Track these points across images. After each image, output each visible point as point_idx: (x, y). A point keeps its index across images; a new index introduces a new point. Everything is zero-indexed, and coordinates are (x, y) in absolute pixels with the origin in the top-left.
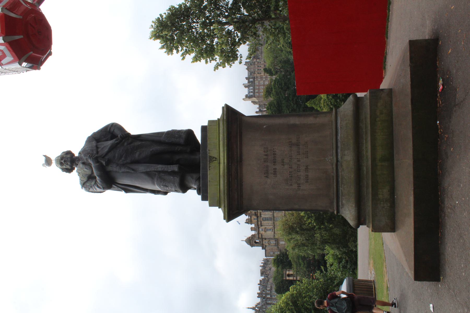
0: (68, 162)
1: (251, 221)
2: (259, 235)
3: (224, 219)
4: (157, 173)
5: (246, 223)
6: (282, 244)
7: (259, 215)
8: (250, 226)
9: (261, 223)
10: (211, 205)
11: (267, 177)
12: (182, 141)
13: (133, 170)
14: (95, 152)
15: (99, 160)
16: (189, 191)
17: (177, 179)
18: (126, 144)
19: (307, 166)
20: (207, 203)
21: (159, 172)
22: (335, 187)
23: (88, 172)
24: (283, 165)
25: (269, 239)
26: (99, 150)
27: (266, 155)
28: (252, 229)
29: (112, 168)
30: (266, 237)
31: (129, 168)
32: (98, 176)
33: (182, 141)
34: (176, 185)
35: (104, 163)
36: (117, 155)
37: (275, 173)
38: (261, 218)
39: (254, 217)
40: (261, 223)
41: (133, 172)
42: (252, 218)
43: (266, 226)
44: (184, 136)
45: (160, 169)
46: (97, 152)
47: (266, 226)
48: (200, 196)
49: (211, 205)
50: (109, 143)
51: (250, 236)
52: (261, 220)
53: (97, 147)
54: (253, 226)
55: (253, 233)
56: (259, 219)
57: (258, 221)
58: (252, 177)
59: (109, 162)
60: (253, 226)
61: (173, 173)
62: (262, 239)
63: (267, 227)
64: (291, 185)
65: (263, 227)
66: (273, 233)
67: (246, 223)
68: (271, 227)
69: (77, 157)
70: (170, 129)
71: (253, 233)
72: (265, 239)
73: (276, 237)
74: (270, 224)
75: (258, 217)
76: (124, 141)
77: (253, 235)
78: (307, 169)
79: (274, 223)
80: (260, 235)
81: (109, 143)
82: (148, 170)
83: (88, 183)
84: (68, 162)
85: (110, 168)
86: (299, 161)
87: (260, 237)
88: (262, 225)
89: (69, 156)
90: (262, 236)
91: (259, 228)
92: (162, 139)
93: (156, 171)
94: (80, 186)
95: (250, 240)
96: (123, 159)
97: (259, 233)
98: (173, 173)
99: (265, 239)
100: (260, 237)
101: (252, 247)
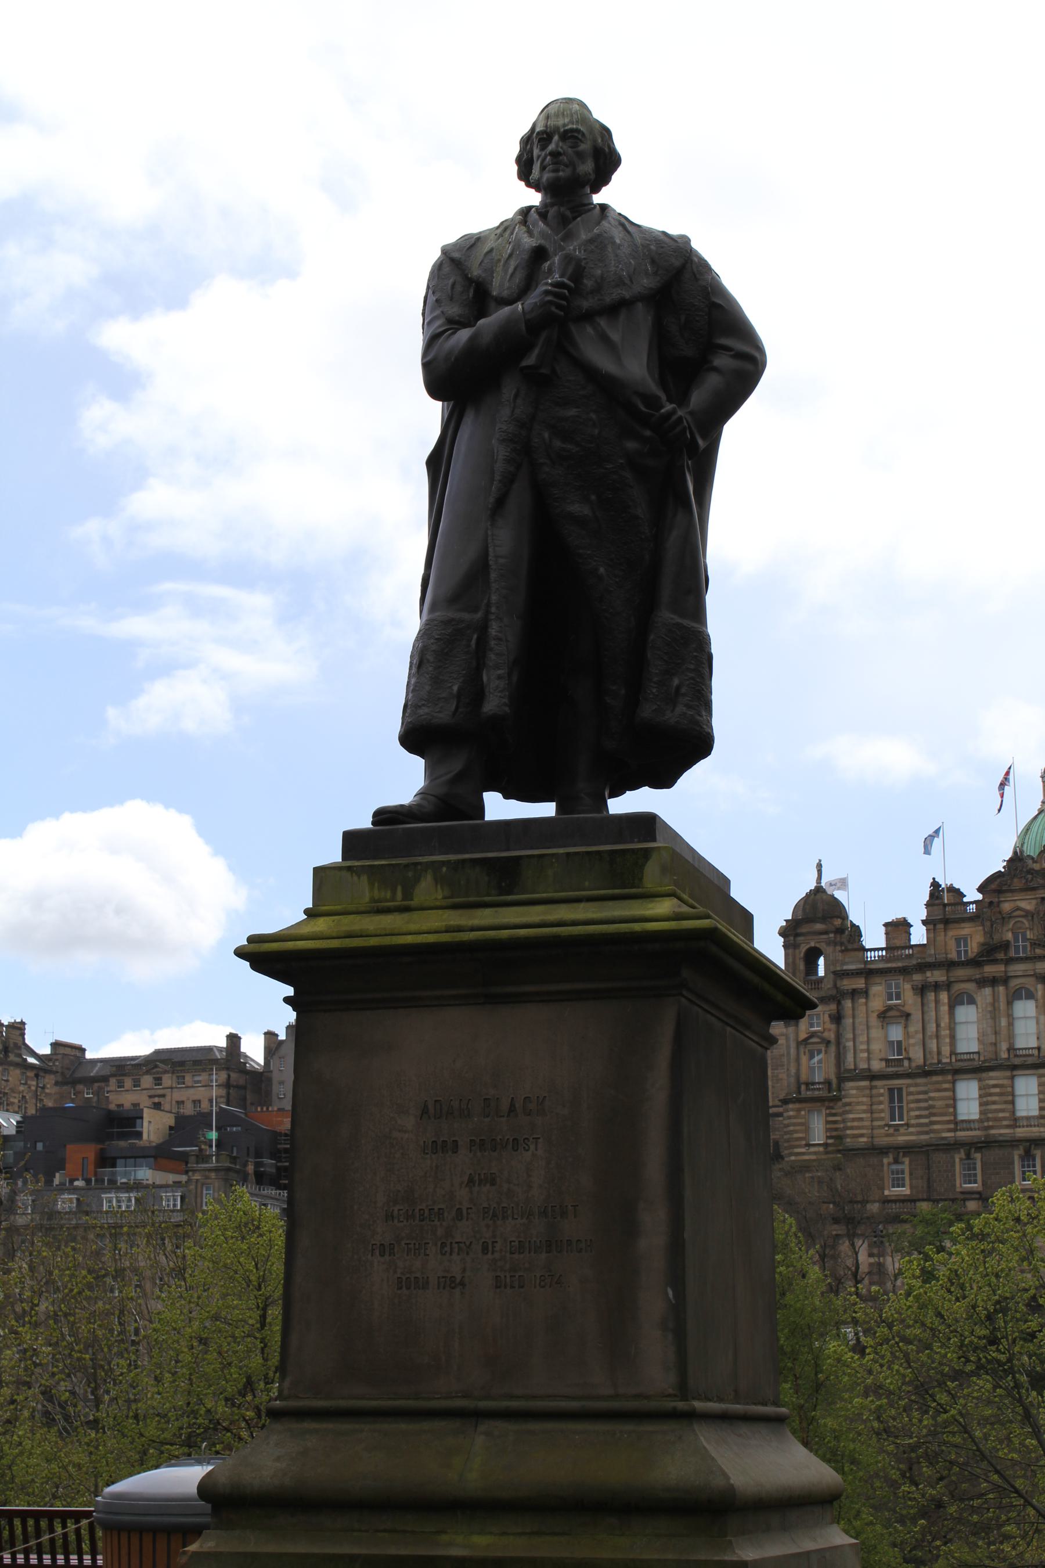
0: (569, 154)
1: (947, 922)
2: (857, 973)
3: (251, 939)
4: (479, 615)
5: (935, 885)
6: (807, 1129)
7: (990, 970)
8: (916, 914)
9: (937, 987)
10: (321, 874)
11: (425, 1111)
12: (647, 711)
13: (500, 503)
14: (586, 304)
15: (544, 335)
16: (418, 763)
17: (443, 714)
18: (631, 445)
19: (462, 1284)
20: (334, 855)
21: (483, 628)
22: (374, 1403)
23: (500, 284)
24: (471, 1181)
25: (839, 1036)
26: (602, 322)
27: (512, 1109)
28: (898, 928)
29: (509, 401)
30: (848, 1021)
31: (509, 481)
32: (472, 339)
33: (647, 711)
34: (426, 710)
35: (531, 360)
36: (572, 412)
37: (442, 1147)
38: (970, 987)
39: (975, 938)
40: (937, 987)
41: (492, 500)
42: (966, 929)
43: (916, 1015)
44: (674, 715)
45: (494, 630)
46: (588, 317)
47: (916, 1015)
48: (365, 822)
49: (321, 874)
50: (633, 365)
51: (855, 916)
52: (957, 987)
53: (613, 310)
54: (919, 935)
55: (874, 938)
56: (961, 973)
57: (950, 965)
58: (429, 1048)
59: (539, 382)
60: (919, 935)
61: (474, 692)
62: (837, 997)
63: (915, 1026)
64: (389, 1217)
65: (909, 999)
66: (877, 1066)
67: (935, 885)
68: (917, 1055)
69: (583, 207)
70: (715, 649)
71: (874, 938)
72: (837, 1018)
73: (853, 1090)
74: (933, 1045)
75: (975, 963)
76: (648, 433)
77: (856, 932)
78: (450, 1283)
79: (942, 1072)
80: (860, 983)
81: (633, 365)
82: (493, 576)
83: (462, 282)
84: (569, 154)
85: (509, 388)
86: (485, 1250)
87: (847, 984)
88: (922, 990)
89: (587, 167)
90: (854, 994)
91: (904, 971)
92: (666, 616)
93: (488, 612)
94: (452, 237)
95: (824, 919)
96: (558, 444)
97: (869, 973)
98: (474, 692)
99: (837, 1018)
100: (847, 984)
101: (783, 932)
